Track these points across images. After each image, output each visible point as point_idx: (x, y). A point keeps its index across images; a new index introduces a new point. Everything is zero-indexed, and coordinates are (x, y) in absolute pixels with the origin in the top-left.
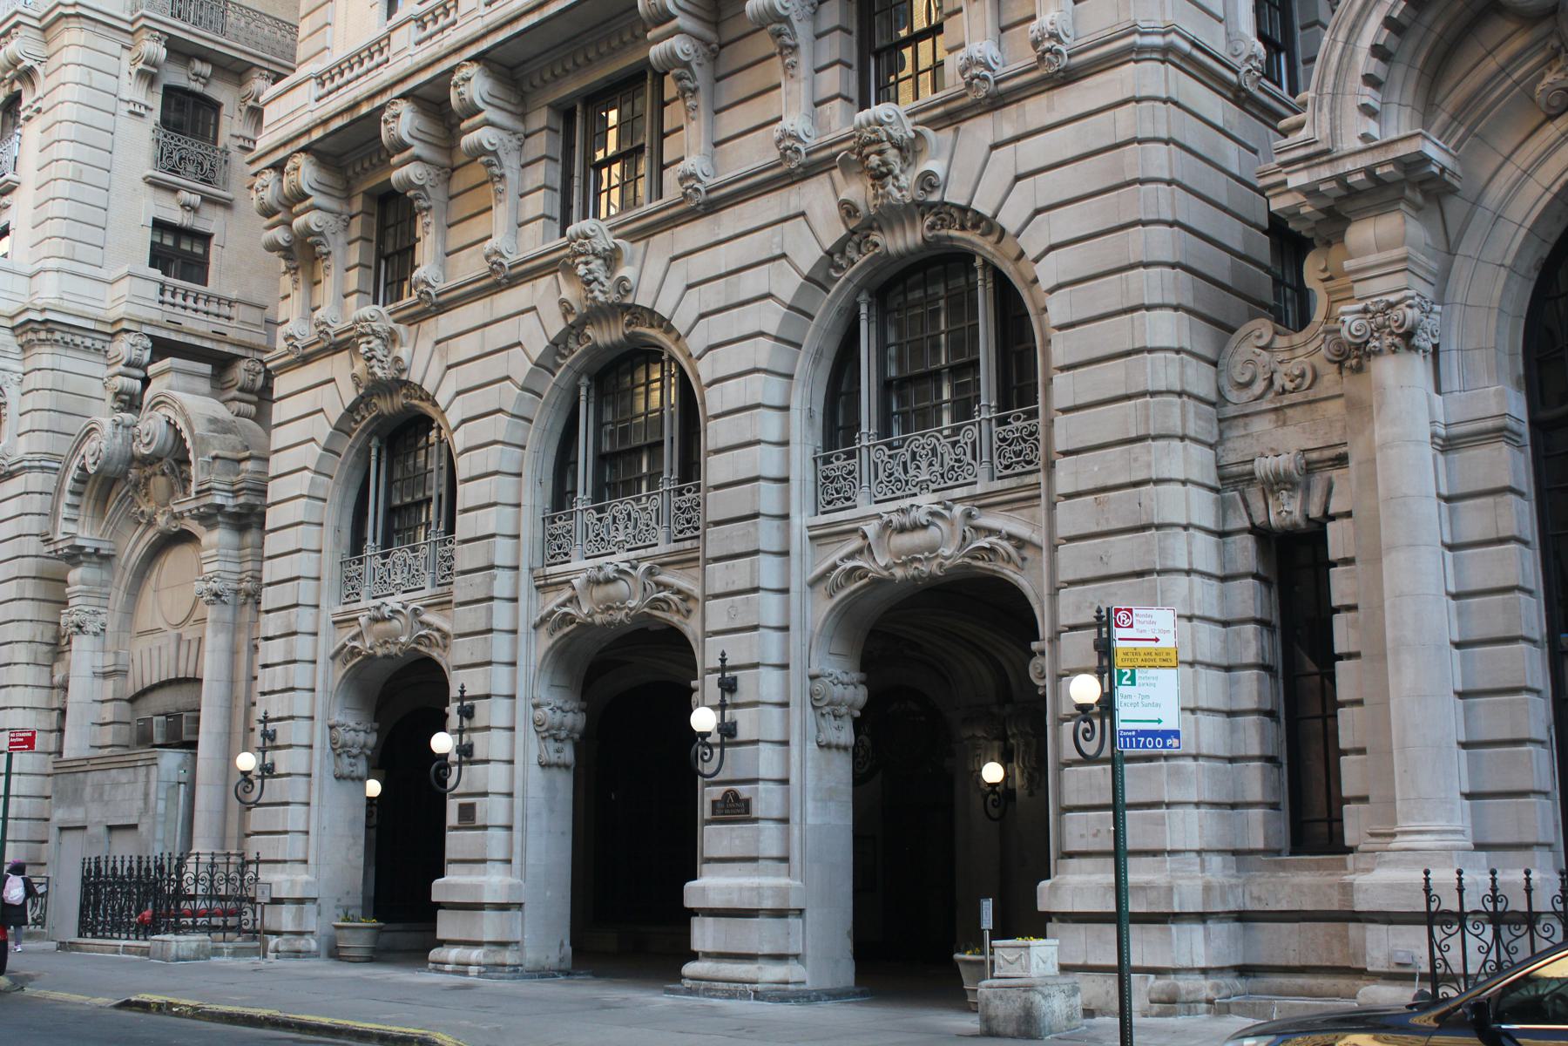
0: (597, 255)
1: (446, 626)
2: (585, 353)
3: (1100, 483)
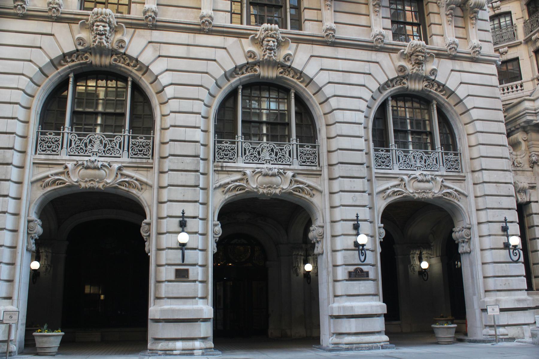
0: (277, 40)
1: (144, 179)
2: (250, 76)
3: (497, 181)
